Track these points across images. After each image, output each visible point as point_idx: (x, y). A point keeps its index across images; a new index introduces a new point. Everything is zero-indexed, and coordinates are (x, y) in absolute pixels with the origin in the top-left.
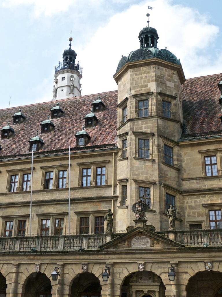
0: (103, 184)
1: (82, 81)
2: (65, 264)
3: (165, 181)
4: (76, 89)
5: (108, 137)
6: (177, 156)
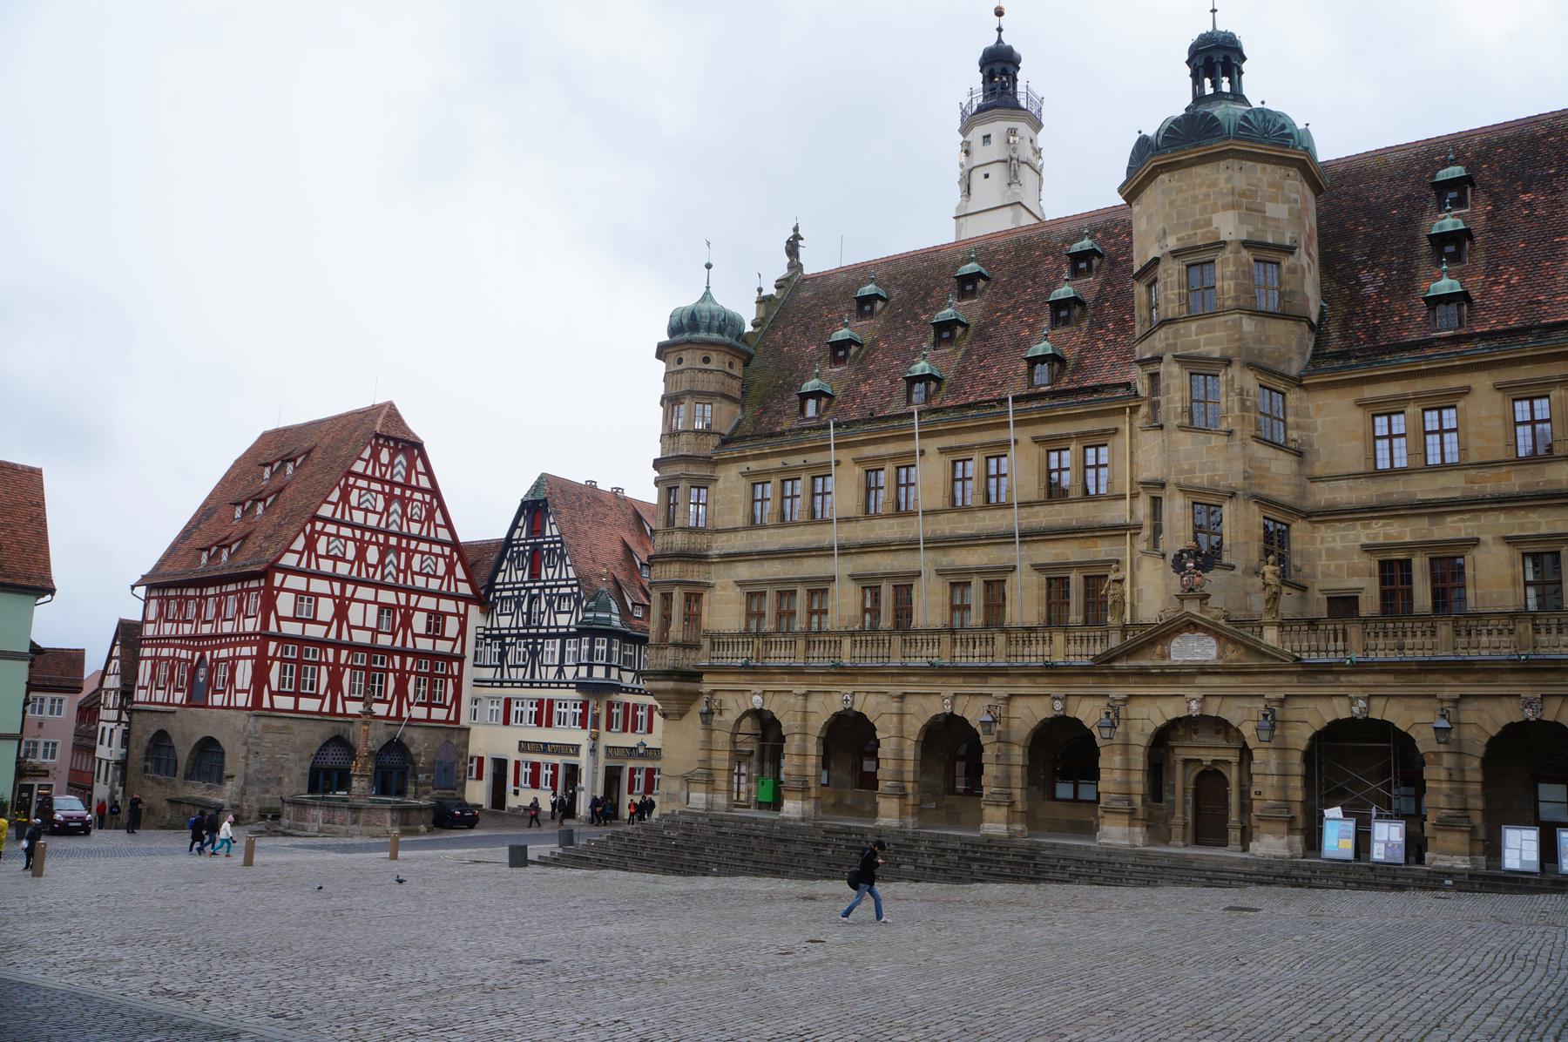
0: (1103, 490)
1: (1042, 139)
2: (1012, 695)
3: (1262, 487)
4: (1025, 169)
5: (1114, 359)
6: (1297, 415)
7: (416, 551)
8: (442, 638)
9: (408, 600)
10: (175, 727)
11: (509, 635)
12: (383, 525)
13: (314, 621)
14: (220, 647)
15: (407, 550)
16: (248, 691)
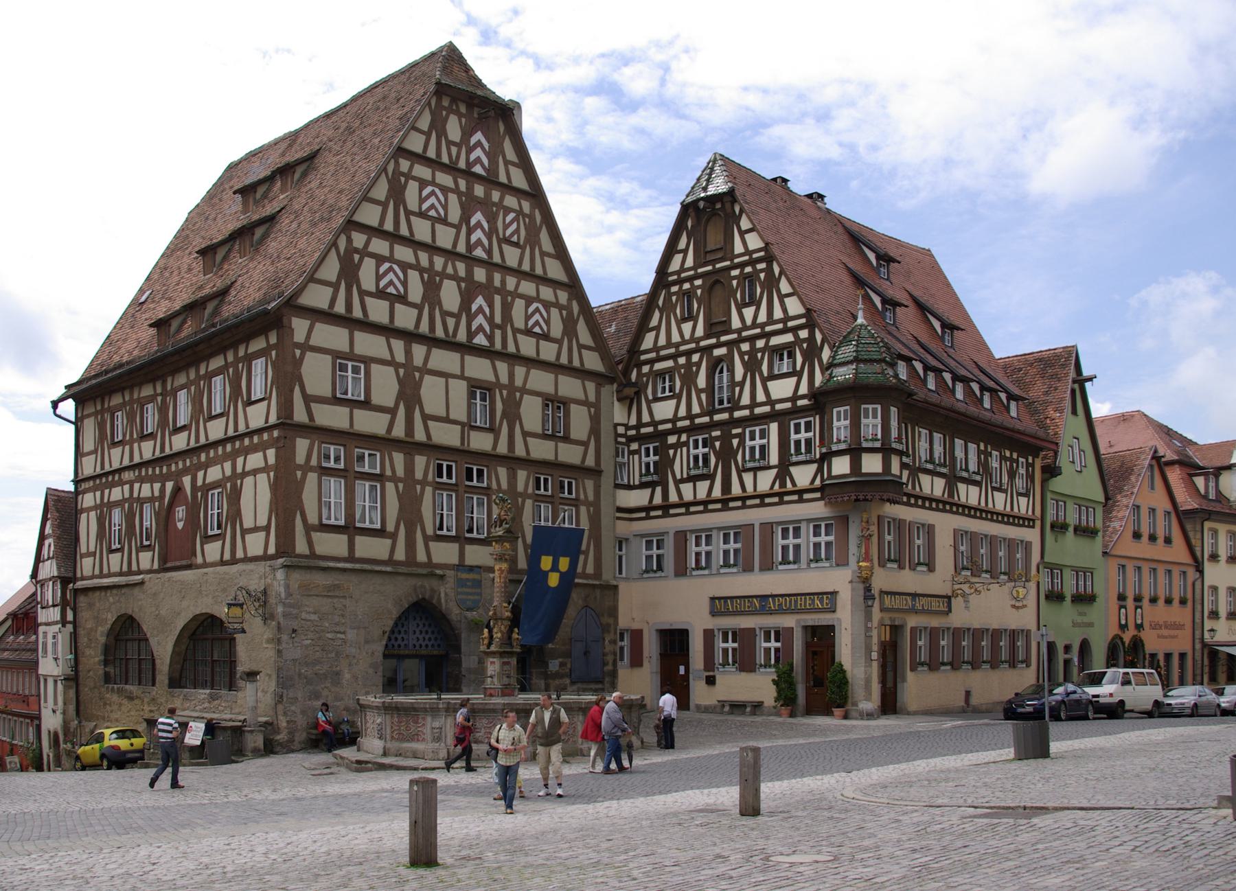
7: (516, 294)
8: (566, 439)
9: (511, 376)
10: (142, 607)
11: (679, 432)
12: (461, 248)
13: (366, 404)
14: (205, 466)
15: (502, 291)
16: (267, 529)
